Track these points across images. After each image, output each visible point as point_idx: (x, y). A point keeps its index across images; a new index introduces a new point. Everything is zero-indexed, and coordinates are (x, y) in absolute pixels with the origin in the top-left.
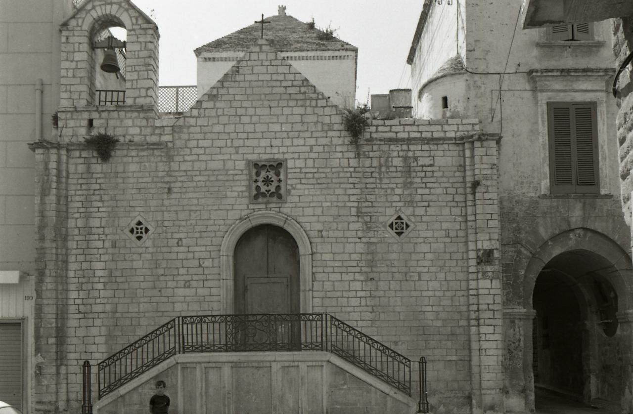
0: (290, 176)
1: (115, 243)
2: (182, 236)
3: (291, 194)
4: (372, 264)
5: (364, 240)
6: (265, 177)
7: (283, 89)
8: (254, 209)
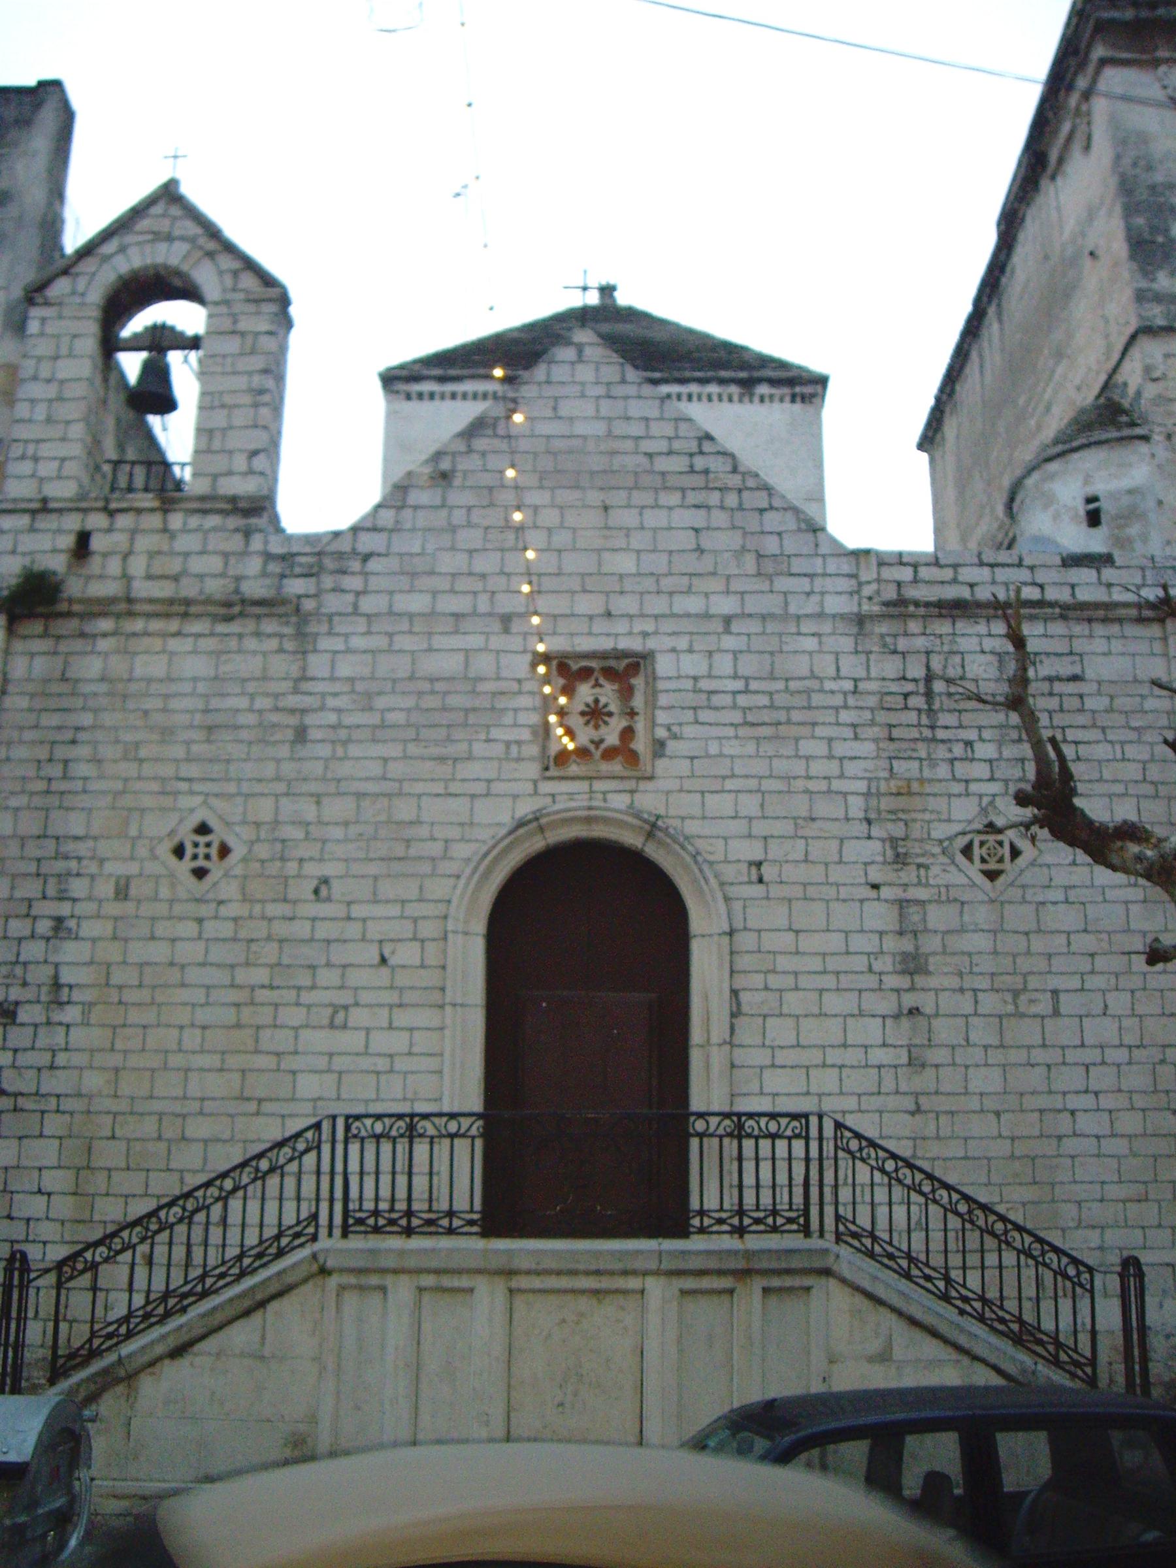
0: (663, 700)
1: (127, 886)
2: (329, 869)
3: (668, 752)
4: (913, 965)
5: (886, 892)
6: (590, 700)
7: (644, 460)
8: (553, 796)
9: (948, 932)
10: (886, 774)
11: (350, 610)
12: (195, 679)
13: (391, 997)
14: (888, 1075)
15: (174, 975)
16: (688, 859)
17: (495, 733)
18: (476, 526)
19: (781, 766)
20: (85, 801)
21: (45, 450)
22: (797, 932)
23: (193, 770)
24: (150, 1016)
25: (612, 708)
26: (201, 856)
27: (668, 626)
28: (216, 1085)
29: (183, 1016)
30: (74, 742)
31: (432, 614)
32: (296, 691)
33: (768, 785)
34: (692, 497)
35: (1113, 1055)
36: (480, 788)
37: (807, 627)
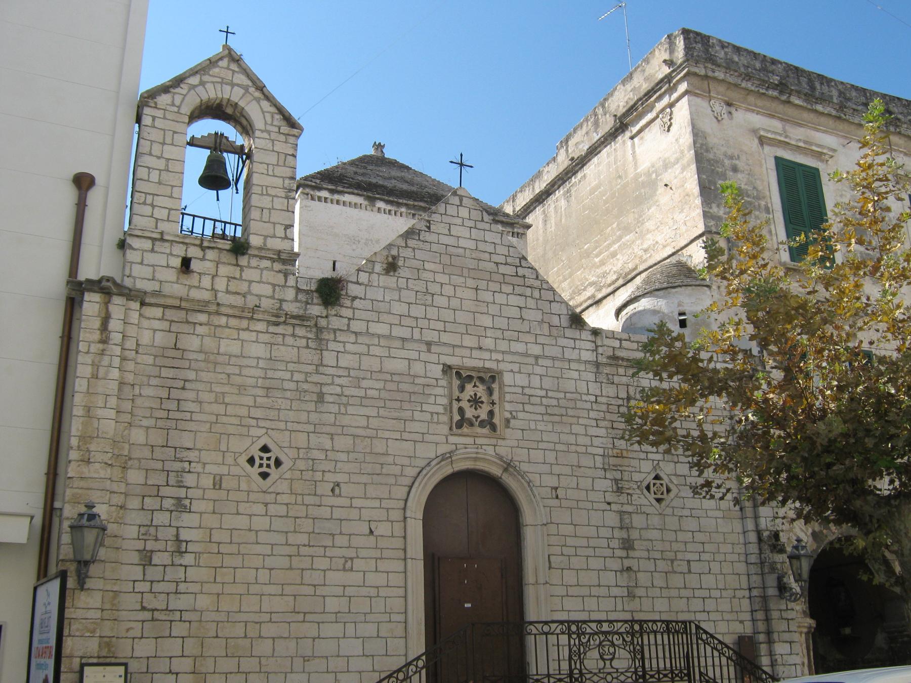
0: (508, 397)
2: (339, 478)
3: (511, 425)
4: (628, 545)
5: (614, 507)
6: (472, 394)
7: (493, 265)
9: (641, 529)
10: (611, 446)
11: (345, 328)
12: (258, 358)
13: (377, 554)
14: (619, 600)
15: (252, 537)
16: (526, 485)
17: (425, 407)
18: (412, 290)
19: (564, 438)
20: (192, 426)
21: (159, 201)
22: (575, 525)
23: (258, 413)
24: (237, 561)
25: (483, 399)
26: (265, 465)
27: (508, 358)
28: (280, 604)
29: (258, 562)
30: (183, 388)
31: (389, 337)
32: (317, 372)
33: (558, 447)
34: (518, 290)
35: (716, 594)
36: (418, 437)
37: (574, 366)
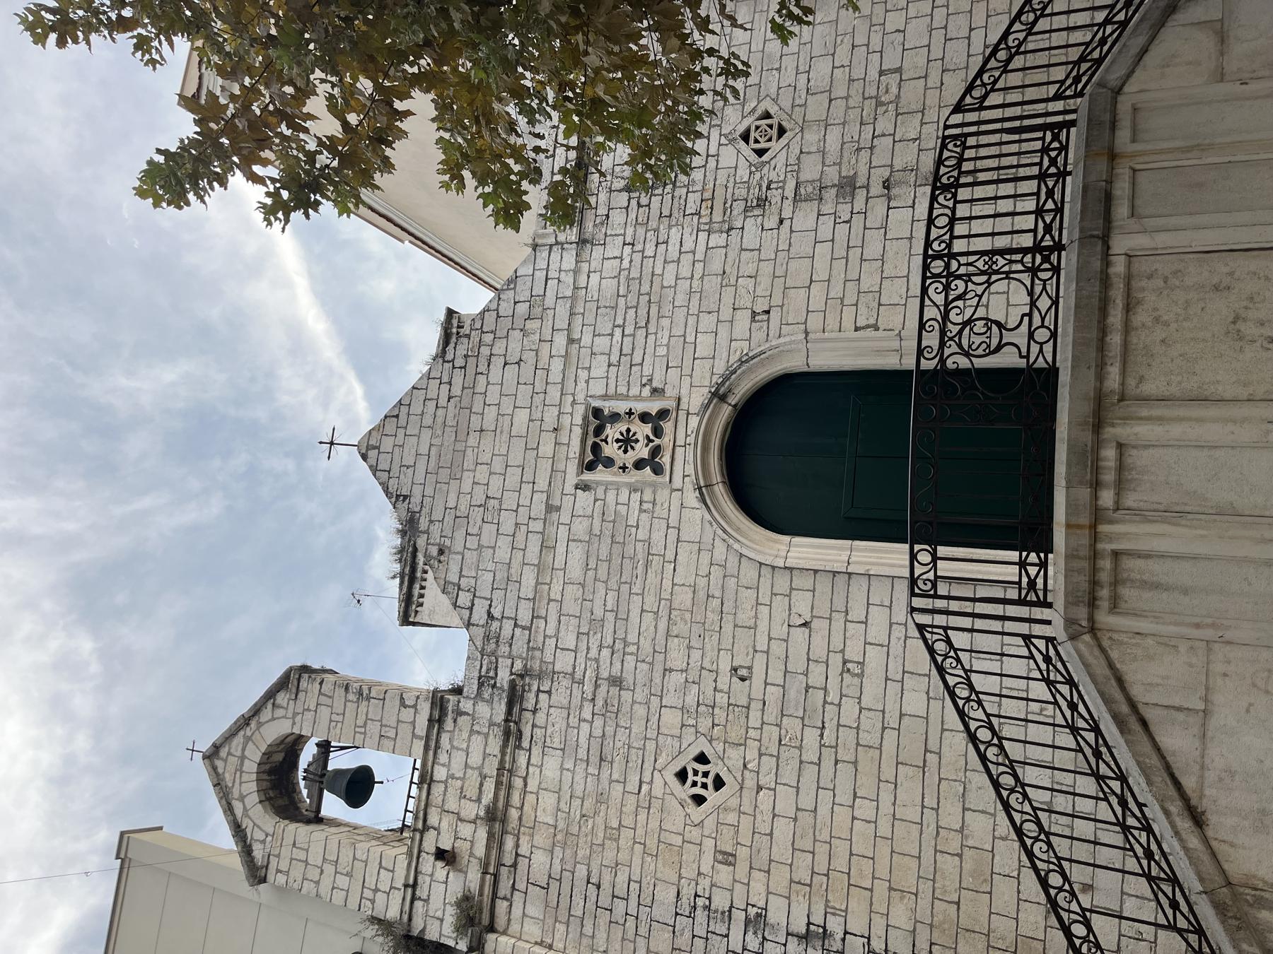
0: (622, 390)
1: (724, 853)
2: (725, 666)
5: (787, 213)
6: (616, 445)
8: (684, 476)
9: (823, 163)
12: (562, 769)
13: (839, 619)
15: (806, 818)
17: (632, 522)
19: (681, 299)
21: (370, 882)
24: (841, 848)
25: (624, 429)
26: (704, 780)
28: (910, 790)
29: (842, 814)
30: (599, 887)
31: (539, 567)
32: (581, 682)
33: (694, 310)
34: (482, 368)
37: (582, 281)
